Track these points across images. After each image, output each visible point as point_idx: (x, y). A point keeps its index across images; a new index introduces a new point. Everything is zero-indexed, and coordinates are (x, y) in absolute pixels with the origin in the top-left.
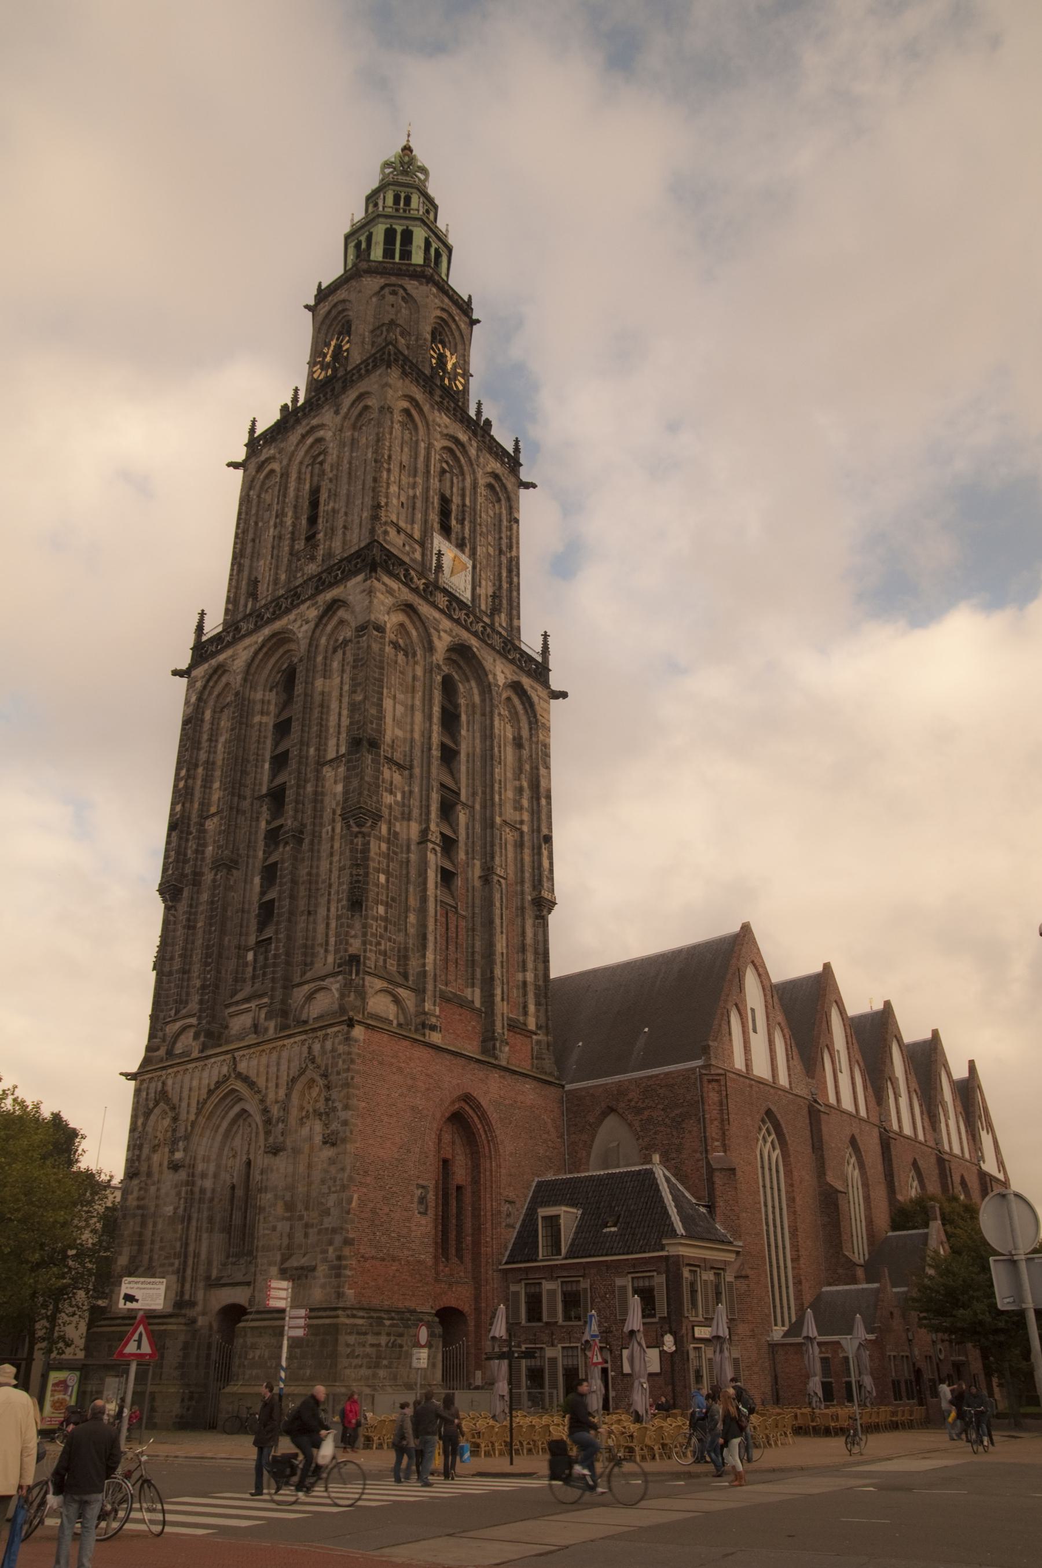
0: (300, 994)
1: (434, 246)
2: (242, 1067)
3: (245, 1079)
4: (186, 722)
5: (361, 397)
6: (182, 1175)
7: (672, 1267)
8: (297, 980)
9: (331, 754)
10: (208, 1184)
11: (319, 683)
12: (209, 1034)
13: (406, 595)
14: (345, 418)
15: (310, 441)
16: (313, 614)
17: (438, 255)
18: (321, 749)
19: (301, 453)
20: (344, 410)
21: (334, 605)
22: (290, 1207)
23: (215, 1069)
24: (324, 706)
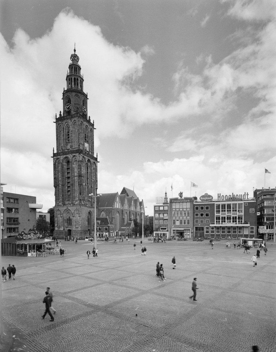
0: (74, 201)
1: (81, 81)
2: (68, 208)
3: (69, 209)
4: (54, 164)
5: (75, 120)
6: (62, 218)
7: (109, 227)
8: (74, 200)
9: (75, 175)
10: (65, 219)
11: (73, 165)
12: (64, 204)
13: (83, 155)
14: (73, 123)
15: (67, 123)
16: (72, 156)
17: (82, 82)
18: (74, 174)
19: (66, 125)
20: (72, 122)
21: (74, 156)
22: (75, 222)
23: (65, 208)
24: (74, 169)
